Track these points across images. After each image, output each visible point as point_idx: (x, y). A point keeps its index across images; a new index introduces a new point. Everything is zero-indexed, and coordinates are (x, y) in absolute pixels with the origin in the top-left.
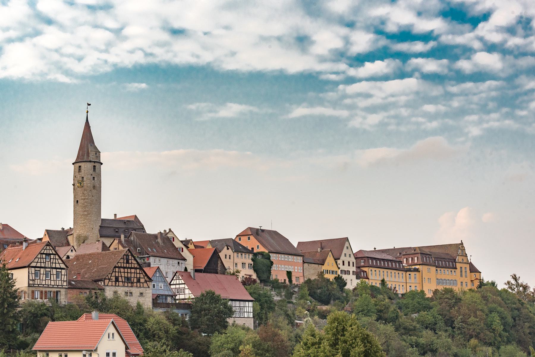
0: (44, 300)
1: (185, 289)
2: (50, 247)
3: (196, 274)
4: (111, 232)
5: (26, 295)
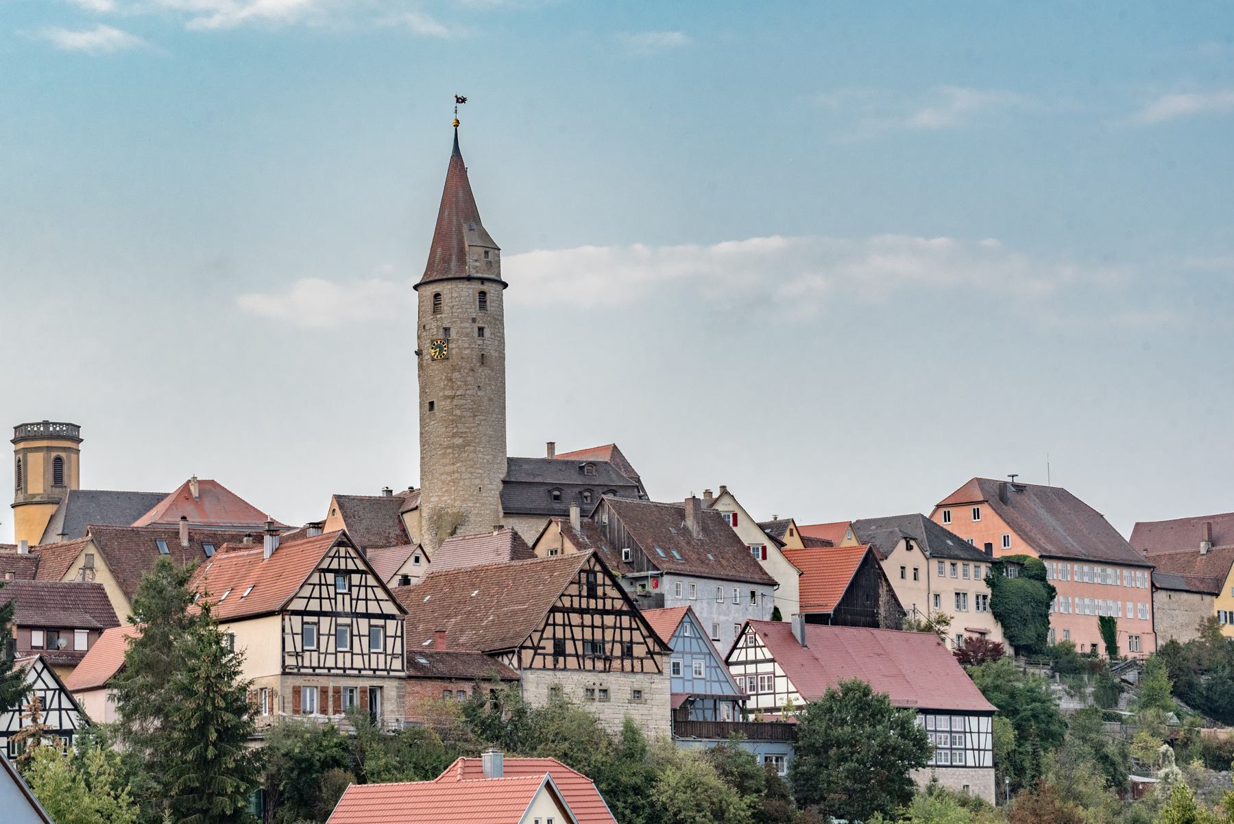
0: (332, 717)
1: (775, 677)
2: (350, 549)
3: (810, 628)
4: (538, 499)
5: (276, 700)
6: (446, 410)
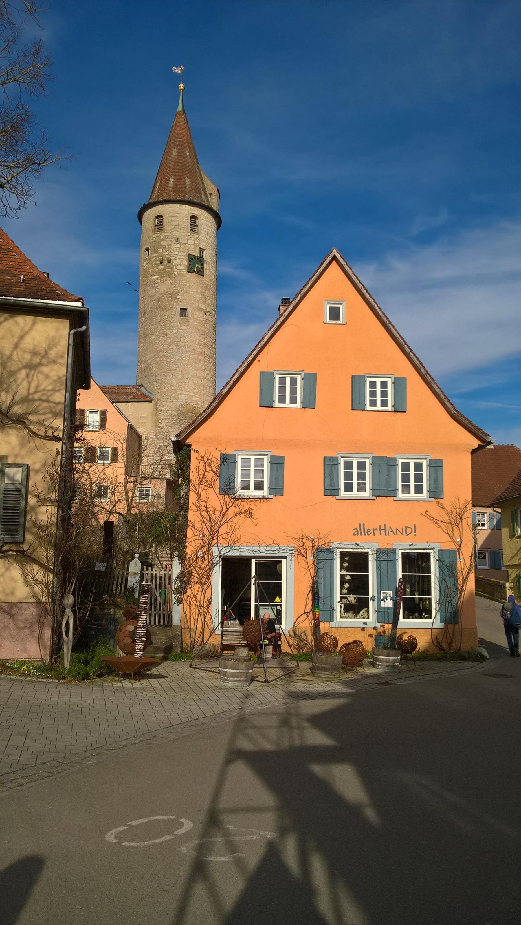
6: (199, 320)
